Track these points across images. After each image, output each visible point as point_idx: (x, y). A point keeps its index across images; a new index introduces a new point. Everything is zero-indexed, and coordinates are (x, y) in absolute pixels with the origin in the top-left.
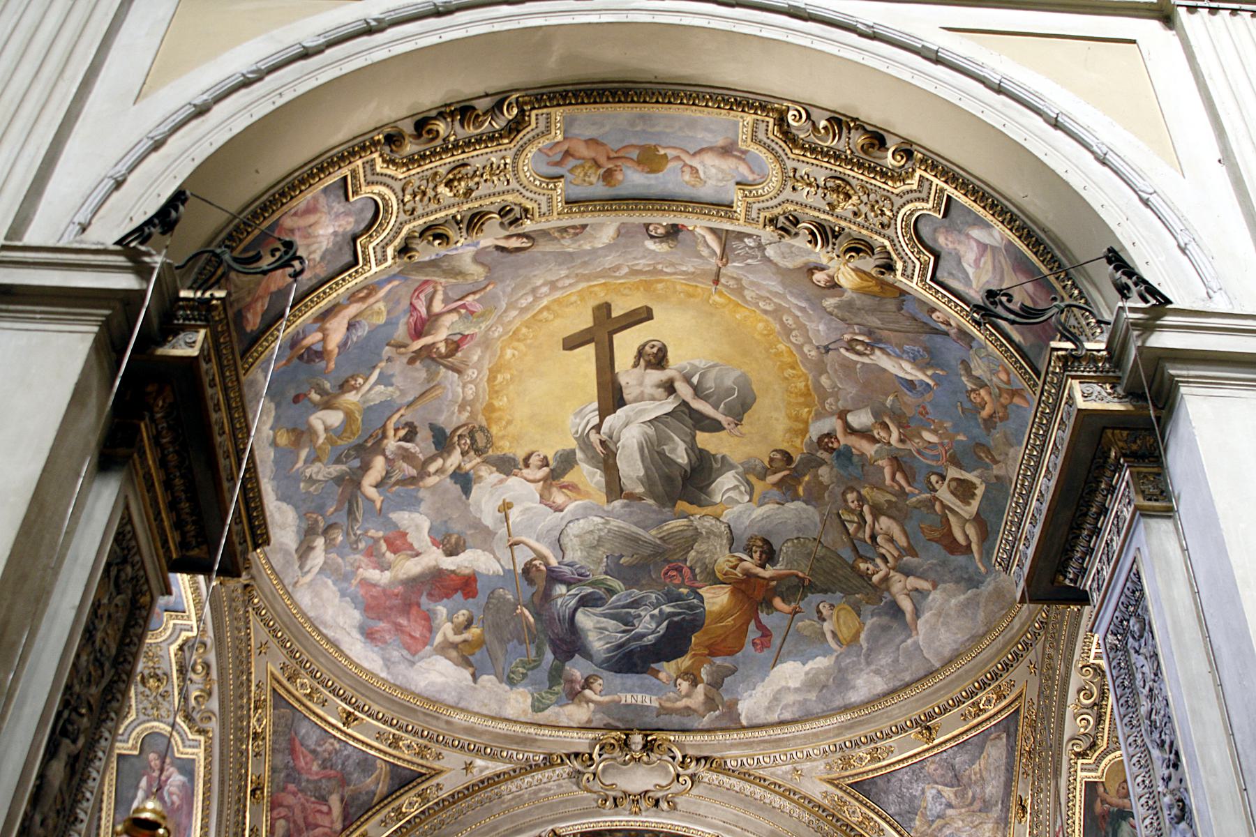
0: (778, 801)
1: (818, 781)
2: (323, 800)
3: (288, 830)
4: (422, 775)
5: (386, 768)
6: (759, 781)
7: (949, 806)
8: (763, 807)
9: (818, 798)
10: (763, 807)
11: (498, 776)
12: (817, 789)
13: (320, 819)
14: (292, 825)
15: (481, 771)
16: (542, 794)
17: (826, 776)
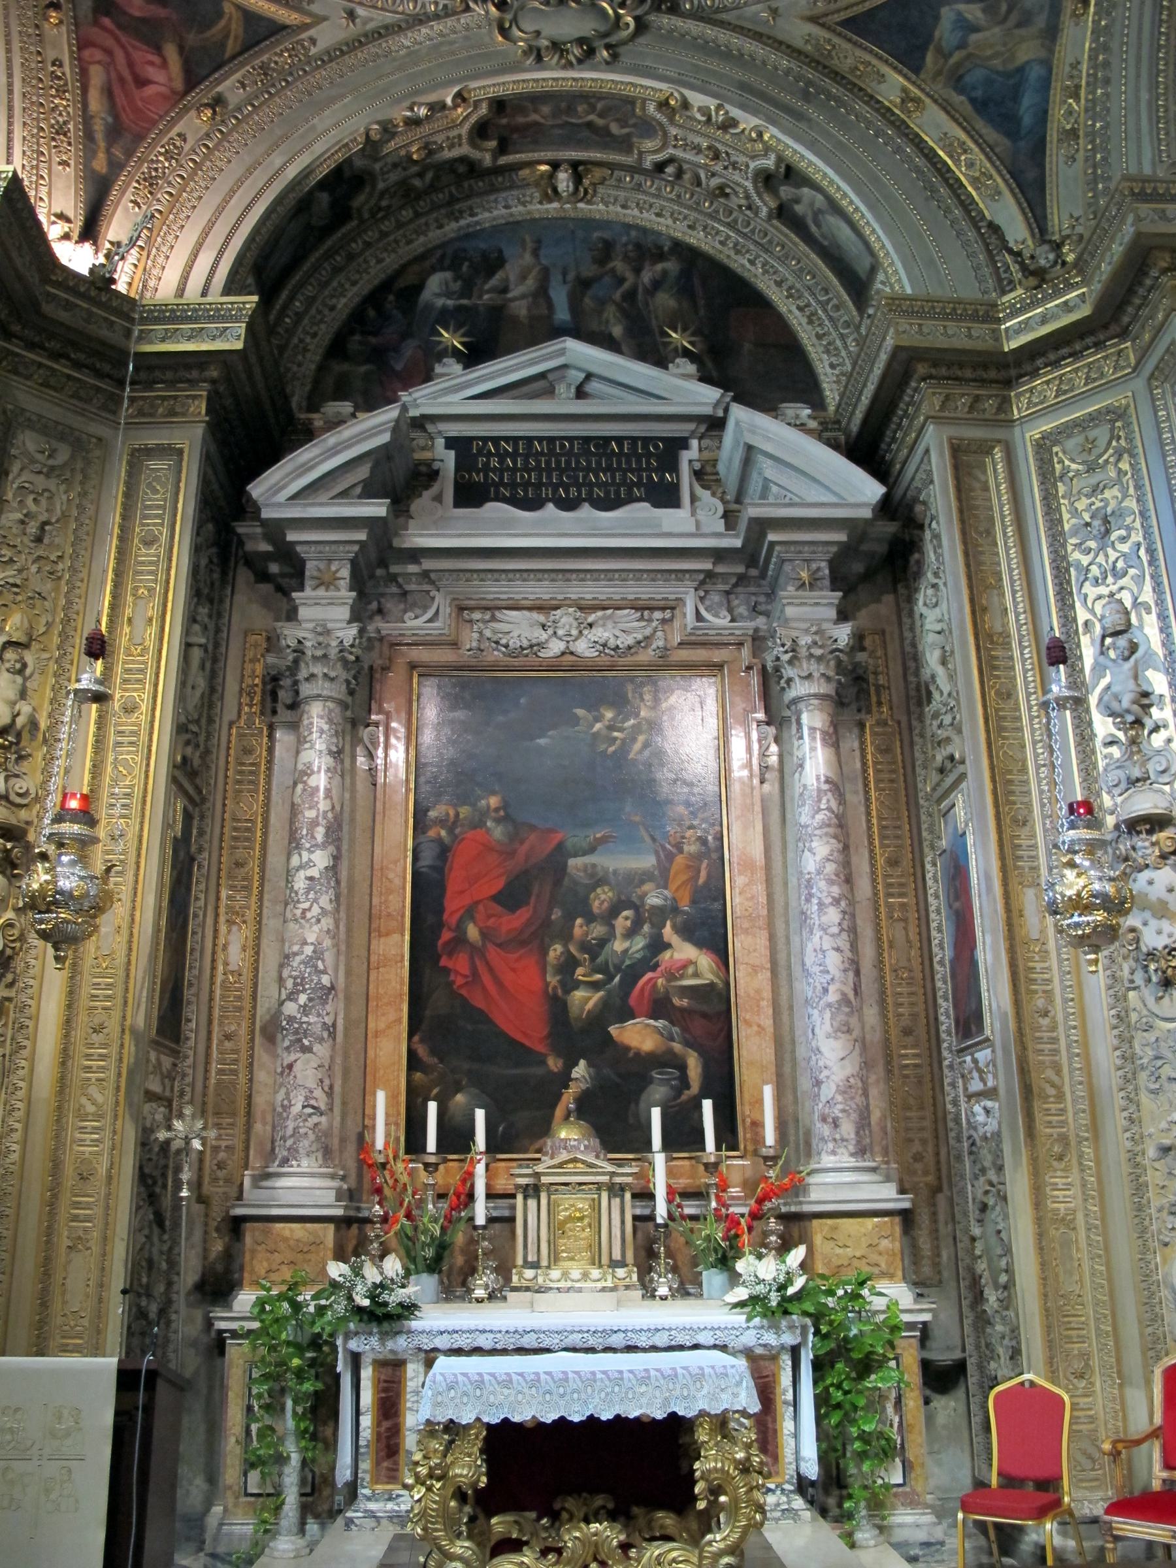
0: (750, 46)
1: (798, 21)
2: (158, 50)
3: (109, 82)
4: (284, 27)
5: (236, 15)
6: (722, 24)
7: (976, 29)
8: (727, 55)
9: (798, 43)
10: (727, 55)
11: (386, 27)
12: (799, 32)
13: (152, 72)
14: (113, 75)
15: (364, 24)
16: (444, 48)
17: (808, 13)
